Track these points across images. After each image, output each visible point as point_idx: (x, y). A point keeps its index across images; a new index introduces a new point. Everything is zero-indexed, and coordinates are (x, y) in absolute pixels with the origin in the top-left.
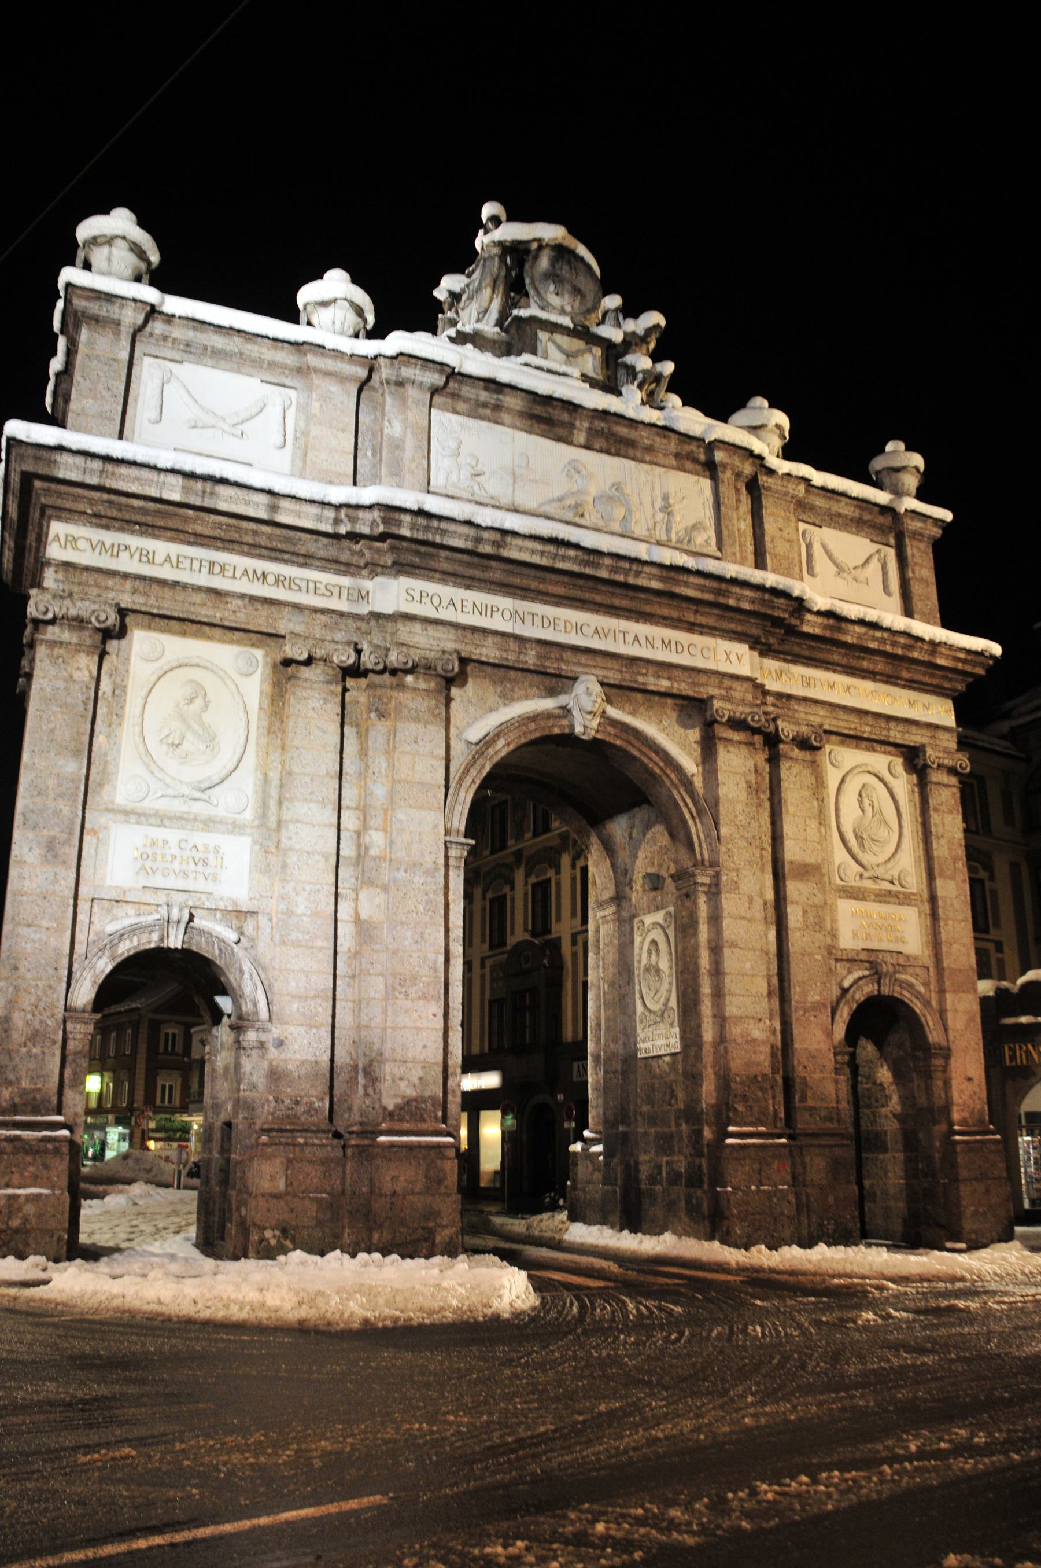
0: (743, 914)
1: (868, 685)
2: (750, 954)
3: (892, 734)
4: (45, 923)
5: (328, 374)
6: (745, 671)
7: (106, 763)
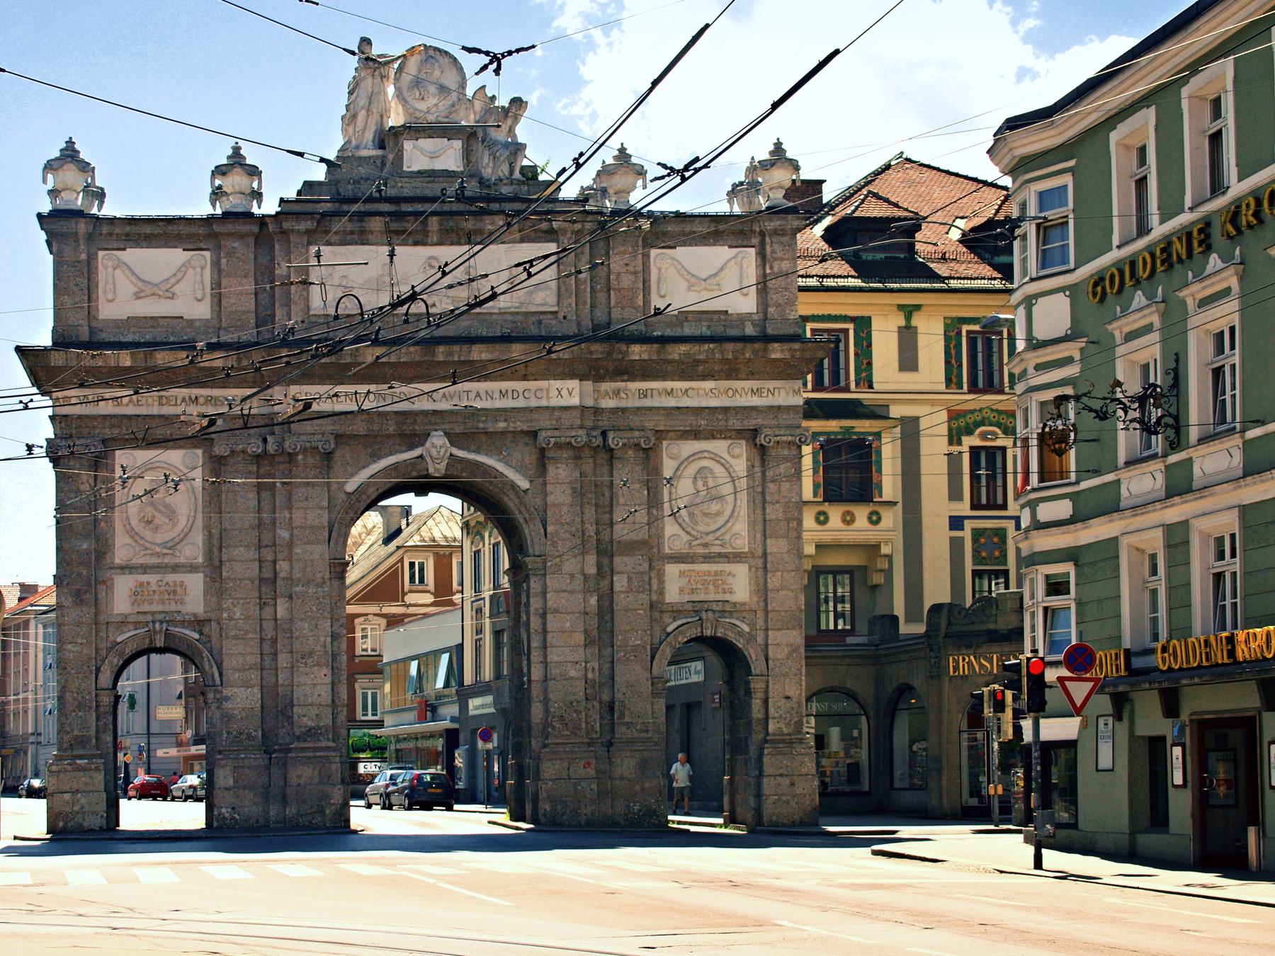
0: (564, 587)
1: (709, 384)
2: (568, 617)
3: (730, 423)
4: (79, 641)
5: (230, 235)
6: (575, 401)
7: (107, 540)
